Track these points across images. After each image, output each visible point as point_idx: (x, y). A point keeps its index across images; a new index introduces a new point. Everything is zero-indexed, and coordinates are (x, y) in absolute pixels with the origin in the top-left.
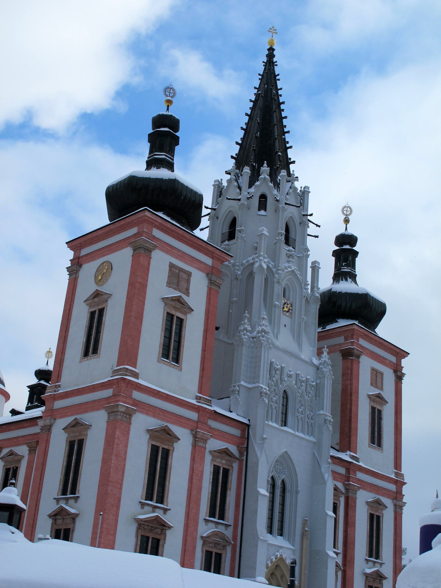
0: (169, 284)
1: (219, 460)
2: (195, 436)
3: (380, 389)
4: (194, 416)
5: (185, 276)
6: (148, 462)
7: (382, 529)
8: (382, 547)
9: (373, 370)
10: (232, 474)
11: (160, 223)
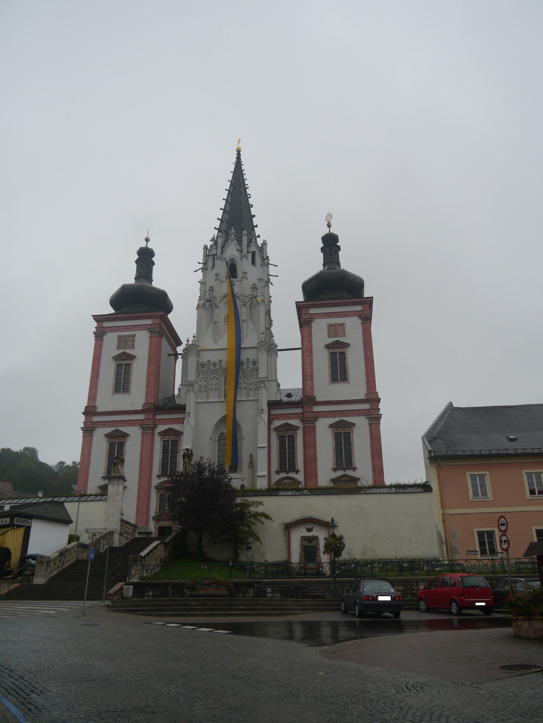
0: (118, 348)
1: (167, 437)
2: (142, 428)
3: (341, 337)
4: (142, 417)
5: (131, 338)
6: (108, 453)
7: (353, 442)
8: (354, 456)
9: (330, 326)
11: (105, 318)
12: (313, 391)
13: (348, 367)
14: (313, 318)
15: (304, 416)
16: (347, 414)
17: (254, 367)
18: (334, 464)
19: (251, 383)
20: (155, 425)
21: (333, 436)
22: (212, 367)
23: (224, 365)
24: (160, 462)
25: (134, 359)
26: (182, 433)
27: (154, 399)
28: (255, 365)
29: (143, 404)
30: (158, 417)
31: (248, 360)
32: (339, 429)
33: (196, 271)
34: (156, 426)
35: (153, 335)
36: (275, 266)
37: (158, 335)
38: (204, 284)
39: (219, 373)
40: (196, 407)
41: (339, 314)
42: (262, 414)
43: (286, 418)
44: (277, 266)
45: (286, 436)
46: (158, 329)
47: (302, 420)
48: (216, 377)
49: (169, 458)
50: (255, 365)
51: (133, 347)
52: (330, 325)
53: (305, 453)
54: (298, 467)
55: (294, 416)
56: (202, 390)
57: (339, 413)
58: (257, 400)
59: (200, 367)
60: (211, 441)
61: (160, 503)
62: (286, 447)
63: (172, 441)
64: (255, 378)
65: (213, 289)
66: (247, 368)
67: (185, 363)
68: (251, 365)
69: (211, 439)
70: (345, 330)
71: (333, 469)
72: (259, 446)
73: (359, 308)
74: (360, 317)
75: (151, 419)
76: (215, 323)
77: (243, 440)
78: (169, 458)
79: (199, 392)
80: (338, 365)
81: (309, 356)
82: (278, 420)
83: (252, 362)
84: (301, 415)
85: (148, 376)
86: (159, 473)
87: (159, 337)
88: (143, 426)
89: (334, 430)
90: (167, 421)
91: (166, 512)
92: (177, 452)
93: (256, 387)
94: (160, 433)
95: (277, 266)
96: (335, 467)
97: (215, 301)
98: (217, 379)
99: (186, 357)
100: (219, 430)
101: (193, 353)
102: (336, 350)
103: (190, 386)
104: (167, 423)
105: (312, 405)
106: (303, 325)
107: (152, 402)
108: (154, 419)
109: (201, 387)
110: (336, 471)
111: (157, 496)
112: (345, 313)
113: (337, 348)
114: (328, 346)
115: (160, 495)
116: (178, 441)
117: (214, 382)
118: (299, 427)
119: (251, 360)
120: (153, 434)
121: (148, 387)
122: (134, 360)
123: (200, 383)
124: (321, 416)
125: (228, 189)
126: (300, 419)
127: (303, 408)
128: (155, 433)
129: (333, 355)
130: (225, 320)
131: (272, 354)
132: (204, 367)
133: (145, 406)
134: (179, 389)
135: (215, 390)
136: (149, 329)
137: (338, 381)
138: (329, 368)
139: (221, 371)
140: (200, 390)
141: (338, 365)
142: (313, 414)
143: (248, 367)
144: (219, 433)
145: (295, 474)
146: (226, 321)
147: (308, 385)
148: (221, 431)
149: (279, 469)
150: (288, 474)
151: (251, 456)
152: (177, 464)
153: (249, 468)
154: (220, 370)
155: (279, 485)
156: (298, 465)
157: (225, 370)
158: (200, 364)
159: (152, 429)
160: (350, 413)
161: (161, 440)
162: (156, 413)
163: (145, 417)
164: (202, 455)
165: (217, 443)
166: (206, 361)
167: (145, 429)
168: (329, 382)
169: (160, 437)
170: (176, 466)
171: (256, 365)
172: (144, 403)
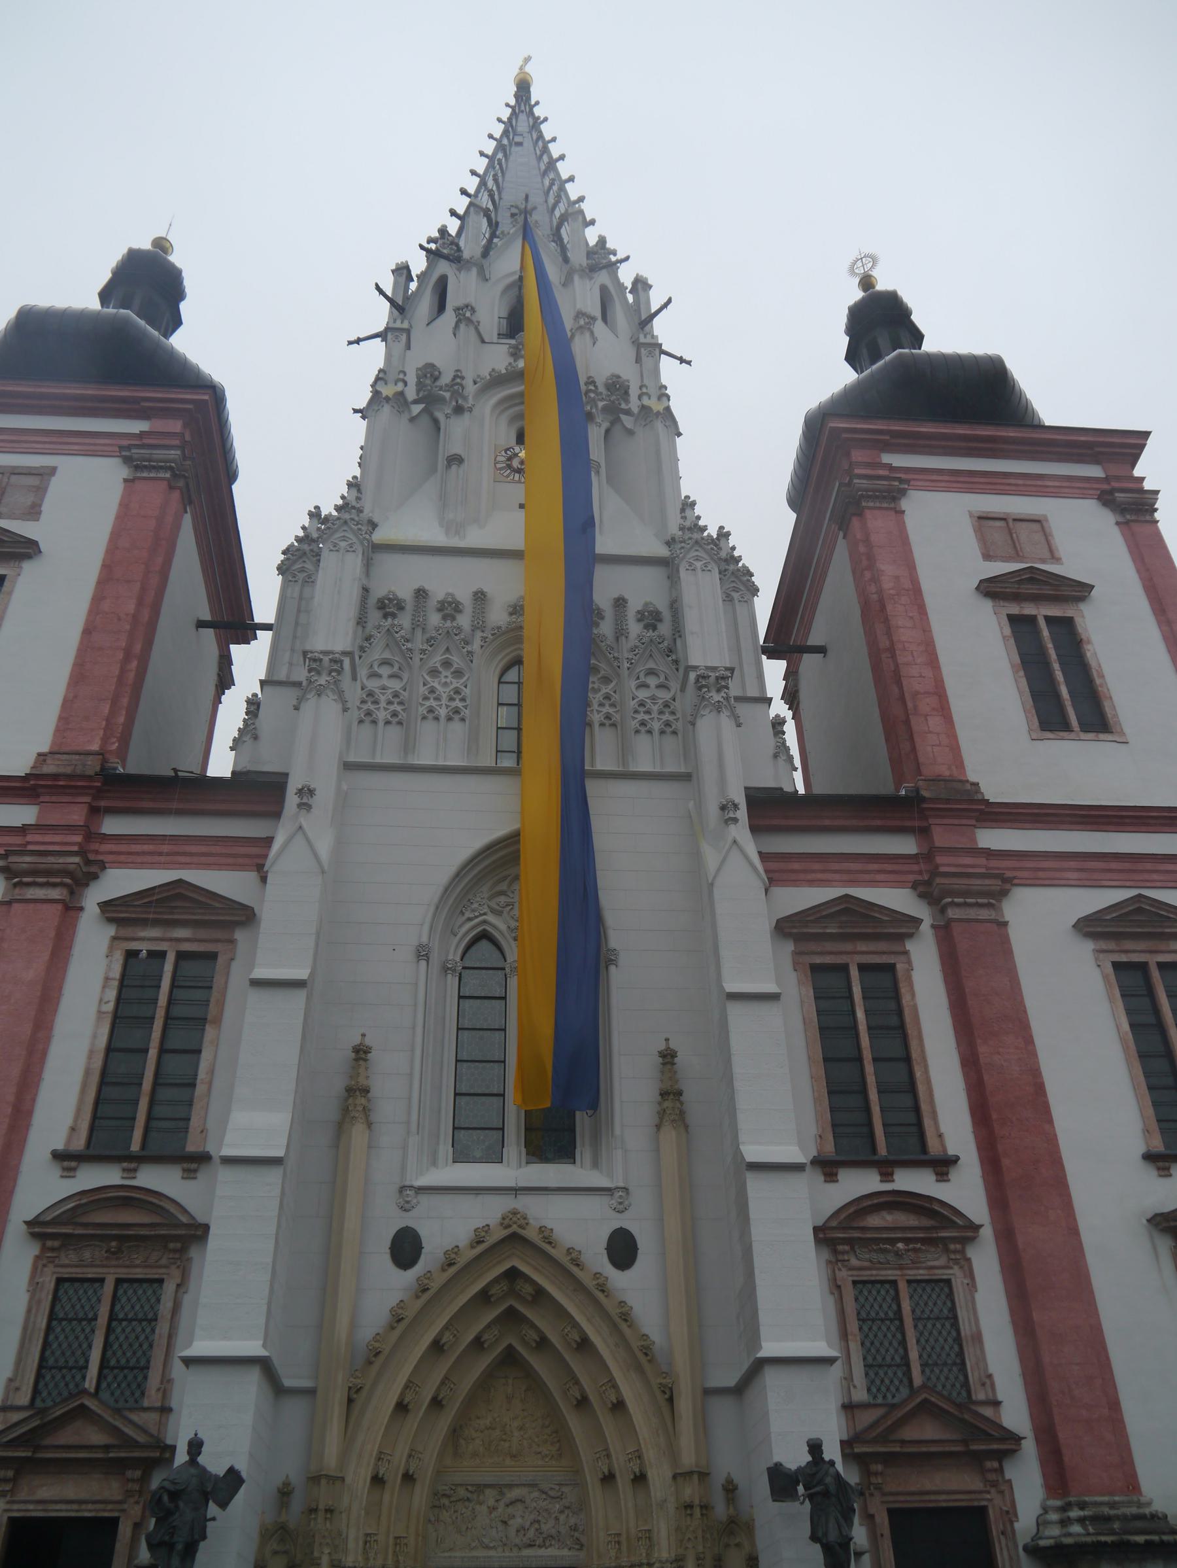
9: (983, 519)
10: (228, 967)
12: (959, 763)
13: (1103, 677)
14: (908, 481)
15: (937, 866)
16: (1155, 876)
17: (650, 634)
18: (1147, 1131)
19: (642, 704)
20: (88, 862)
21: (1105, 977)
22: (434, 619)
23: (498, 616)
24: (87, 1072)
25: (29, 557)
26: (245, 916)
27: (105, 740)
28: (654, 628)
29: (40, 755)
30: (112, 826)
31: (620, 603)
32: (1129, 945)
33: (358, 341)
34: (93, 869)
35: (145, 475)
36: (682, 360)
37: (168, 475)
38: (404, 337)
39: (476, 645)
40: (345, 787)
41: (1012, 481)
42: (732, 827)
43: (837, 876)
44: (689, 363)
45: (844, 969)
46: (173, 452)
47: (926, 891)
48: (457, 661)
49: (153, 1053)
50: (654, 628)
51: (33, 512)
52: (985, 515)
53: (971, 1063)
54: (940, 1136)
55: (879, 872)
56: (382, 715)
57: (1114, 865)
58: (686, 777)
59: (374, 616)
60: (423, 963)
61: (46, 1345)
62: (855, 1027)
63: (181, 956)
64: (659, 686)
65: (437, 373)
66: (617, 639)
67: (296, 595)
68: (635, 629)
69: (423, 953)
70: (1050, 538)
71: (1149, 1157)
72: (731, 987)
73: (1095, 471)
74: (1107, 499)
75: (70, 828)
76: (455, 460)
77: (612, 968)
78: (153, 1053)
79: (361, 721)
80: (1056, 666)
81: (911, 618)
82: (795, 883)
83: (641, 616)
84: (915, 868)
85: (87, 631)
86: (69, 1140)
87: (171, 488)
88: (12, 859)
89: (1103, 945)
90: (166, 848)
91: (82, 1406)
92: (206, 1019)
93: (668, 724)
94: (112, 910)
95: (689, 363)
96: (1158, 1145)
97: (458, 384)
98: (458, 673)
99: (302, 570)
100: (464, 918)
101: (344, 538)
102: (1029, 609)
103: (319, 673)
104: (163, 859)
105: (973, 822)
106: (864, 504)
107: (95, 747)
108: (91, 835)
109: (376, 702)
110: (1168, 1169)
111: (34, 1286)
112: (1039, 483)
113: (1036, 599)
114: (991, 589)
115: (60, 1281)
116: (221, 960)
117: (446, 684)
118: (917, 922)
119: (634, 606)
120: (71, 909)
121: (79, 676)
122: (27, 566)
123: (372, 684)
124: (1025, 874)
125: (498, 137)
126: (914, 886)
127: (923, 832)
128: (81, 909)
129: (1021, 626)
130: (499, 466)
131: (736, 595)
132: (394, 616)
133: (49, 762)
134: (249, 702)
135: (450, 719)
136: (129, 448)
137: (1067, 727)
138: (1015, 672)
139: (484, 639)
140: (369, 713)
141: (1056, 666)
142: (982, 861)
143: (620, 632)
144: (466, 930)
145: (934, 1177)
146: (501, 469)
147: (930, 732)
148: (476, 921)
149: (830, 1148)
150: (887, 1176)
151: (668, 1057)
152: (200, 1089)
153: (658, 1127)
154: (479, 634)
155: (844, 1241)
156: (943, 1129)
157: (512, 636)
158: (372, 601)
159: (68, 881)
160: (1168, 872)
161: (111, 949)
162: (103, 803)
163: (38, 818)
164: (363, 1035)
165: (452, 981)
166: (405, 593)
167: (25, 880)
168: (1030, 730)
169: (111, 930)
170: (190, 1104)
171: (665, 629)
172: (45, 749)
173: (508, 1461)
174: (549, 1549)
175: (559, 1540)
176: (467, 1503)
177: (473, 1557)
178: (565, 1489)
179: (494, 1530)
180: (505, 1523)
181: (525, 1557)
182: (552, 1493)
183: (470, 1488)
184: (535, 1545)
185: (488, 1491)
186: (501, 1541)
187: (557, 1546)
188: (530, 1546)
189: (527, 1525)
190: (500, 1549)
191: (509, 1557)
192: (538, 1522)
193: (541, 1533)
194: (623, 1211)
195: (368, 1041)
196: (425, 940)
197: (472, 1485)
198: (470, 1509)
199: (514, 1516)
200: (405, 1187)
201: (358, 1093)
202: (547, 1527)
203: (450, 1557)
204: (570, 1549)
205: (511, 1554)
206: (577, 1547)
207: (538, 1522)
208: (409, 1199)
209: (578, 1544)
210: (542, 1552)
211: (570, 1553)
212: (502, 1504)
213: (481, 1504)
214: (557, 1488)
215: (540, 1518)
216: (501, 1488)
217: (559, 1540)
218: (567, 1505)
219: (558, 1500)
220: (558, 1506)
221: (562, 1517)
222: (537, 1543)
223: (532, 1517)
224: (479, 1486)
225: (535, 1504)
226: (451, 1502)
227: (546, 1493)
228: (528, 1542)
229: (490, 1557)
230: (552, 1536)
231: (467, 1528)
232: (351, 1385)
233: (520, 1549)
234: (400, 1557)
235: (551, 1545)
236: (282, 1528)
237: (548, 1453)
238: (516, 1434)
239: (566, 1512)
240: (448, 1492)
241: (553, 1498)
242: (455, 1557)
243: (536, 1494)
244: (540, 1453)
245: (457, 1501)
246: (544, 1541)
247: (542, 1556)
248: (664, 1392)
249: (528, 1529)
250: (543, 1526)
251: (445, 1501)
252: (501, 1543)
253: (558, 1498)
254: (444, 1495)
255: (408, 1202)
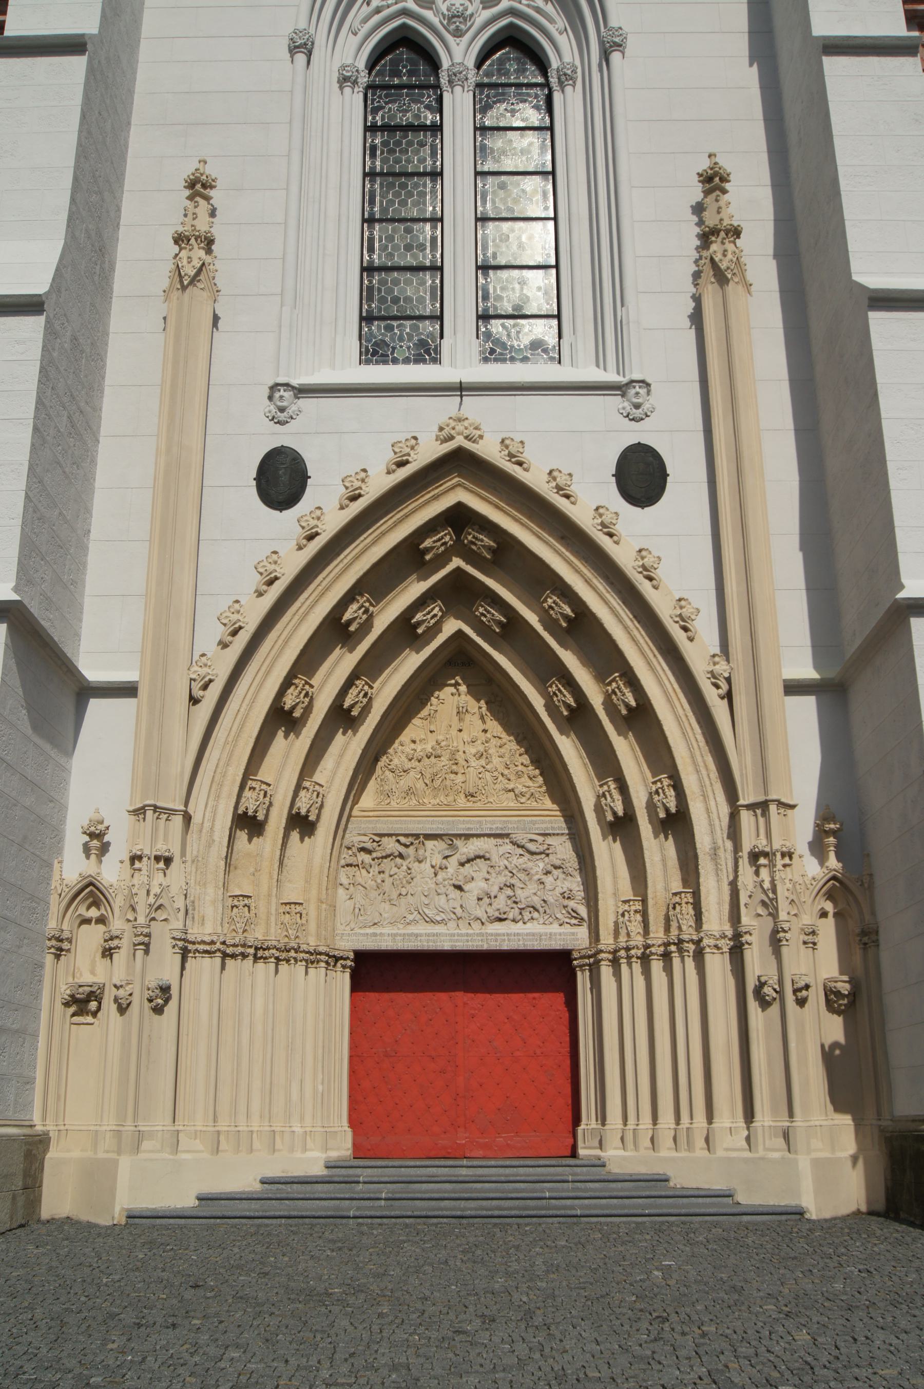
173: (462, 801)
174: (529, 925)
175: (545, 912)
176: (398, 860)
177: (409, 935)
178: (550, 840)
179: (443, 897)
180: (459, 888)
181: (492, 935)
182: (532, 847)
183: (402, 839)
184: (505, 919)
185: (430, 844)
186: (454, 913)
187: (541, 921)
188: (500, 920)
189: (494, 890)
190: (452, 924)
191: (467, 935)
192: (512, 886)
193: (516, 902)
194: (642, 419)
195: (211, 170)
196: (302, 25)
197: (406, 835)
198: (405, 868)
199: (473, 879)
200: (278, 385)
201: (193, 241)
202: (527, 893)
203: (375, 935)
204: (561, 925)
205: (471, 931)
206: (574, 921)
207: (512, 886)
208: (285, 404)
209: (576, 918)
210: (519, 928)
211: (562, 930)
212: (453, 862)
213: (420, 862)
214: (540, 839)
215: (513, 881)
216: (449, 838)
217: (545, 912)
218: (558, 863)
219: (543, 856)
220: (541, 865)
221: (549, 880)
222: (511, 916)
223: (502, 879)
224: (417, 836)
225: (506, 862)
226: (373, 860)
227: (523, 847)
228: (497, 914)
229: (437, 935)
230: (533, 907)
231: (400, 894)
232: (193, 676)
233: (483, 924)
234: (290, 932)
235: (532, 918)
236: (91, 884)
237: (524, 790)
238: (474, 763)
239: (556, 872)
240: (369, 845)
241: (532, 853)
242: (381, 934)
243: (509, 847)
244: (512, 790)
245: (383, 857)
246: (521, 913)
247: (518, 934)
248: (717, 686)
249: (495, 897)
250: (519, 892)
251: (367, 858)
252: (453, 916)
253: (541, 853)
254: (363, 849)
255: (282, 410)
